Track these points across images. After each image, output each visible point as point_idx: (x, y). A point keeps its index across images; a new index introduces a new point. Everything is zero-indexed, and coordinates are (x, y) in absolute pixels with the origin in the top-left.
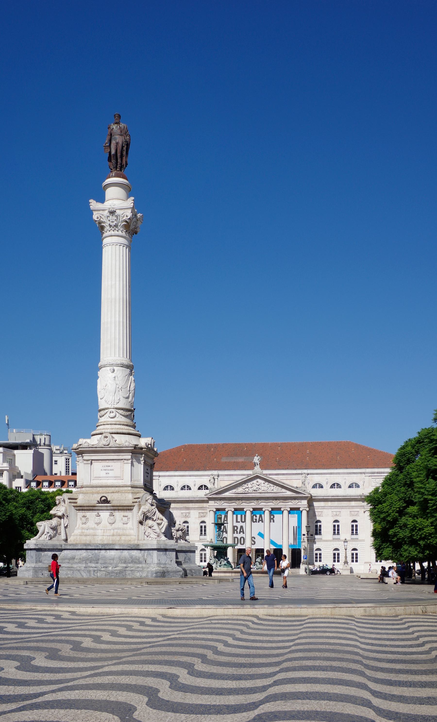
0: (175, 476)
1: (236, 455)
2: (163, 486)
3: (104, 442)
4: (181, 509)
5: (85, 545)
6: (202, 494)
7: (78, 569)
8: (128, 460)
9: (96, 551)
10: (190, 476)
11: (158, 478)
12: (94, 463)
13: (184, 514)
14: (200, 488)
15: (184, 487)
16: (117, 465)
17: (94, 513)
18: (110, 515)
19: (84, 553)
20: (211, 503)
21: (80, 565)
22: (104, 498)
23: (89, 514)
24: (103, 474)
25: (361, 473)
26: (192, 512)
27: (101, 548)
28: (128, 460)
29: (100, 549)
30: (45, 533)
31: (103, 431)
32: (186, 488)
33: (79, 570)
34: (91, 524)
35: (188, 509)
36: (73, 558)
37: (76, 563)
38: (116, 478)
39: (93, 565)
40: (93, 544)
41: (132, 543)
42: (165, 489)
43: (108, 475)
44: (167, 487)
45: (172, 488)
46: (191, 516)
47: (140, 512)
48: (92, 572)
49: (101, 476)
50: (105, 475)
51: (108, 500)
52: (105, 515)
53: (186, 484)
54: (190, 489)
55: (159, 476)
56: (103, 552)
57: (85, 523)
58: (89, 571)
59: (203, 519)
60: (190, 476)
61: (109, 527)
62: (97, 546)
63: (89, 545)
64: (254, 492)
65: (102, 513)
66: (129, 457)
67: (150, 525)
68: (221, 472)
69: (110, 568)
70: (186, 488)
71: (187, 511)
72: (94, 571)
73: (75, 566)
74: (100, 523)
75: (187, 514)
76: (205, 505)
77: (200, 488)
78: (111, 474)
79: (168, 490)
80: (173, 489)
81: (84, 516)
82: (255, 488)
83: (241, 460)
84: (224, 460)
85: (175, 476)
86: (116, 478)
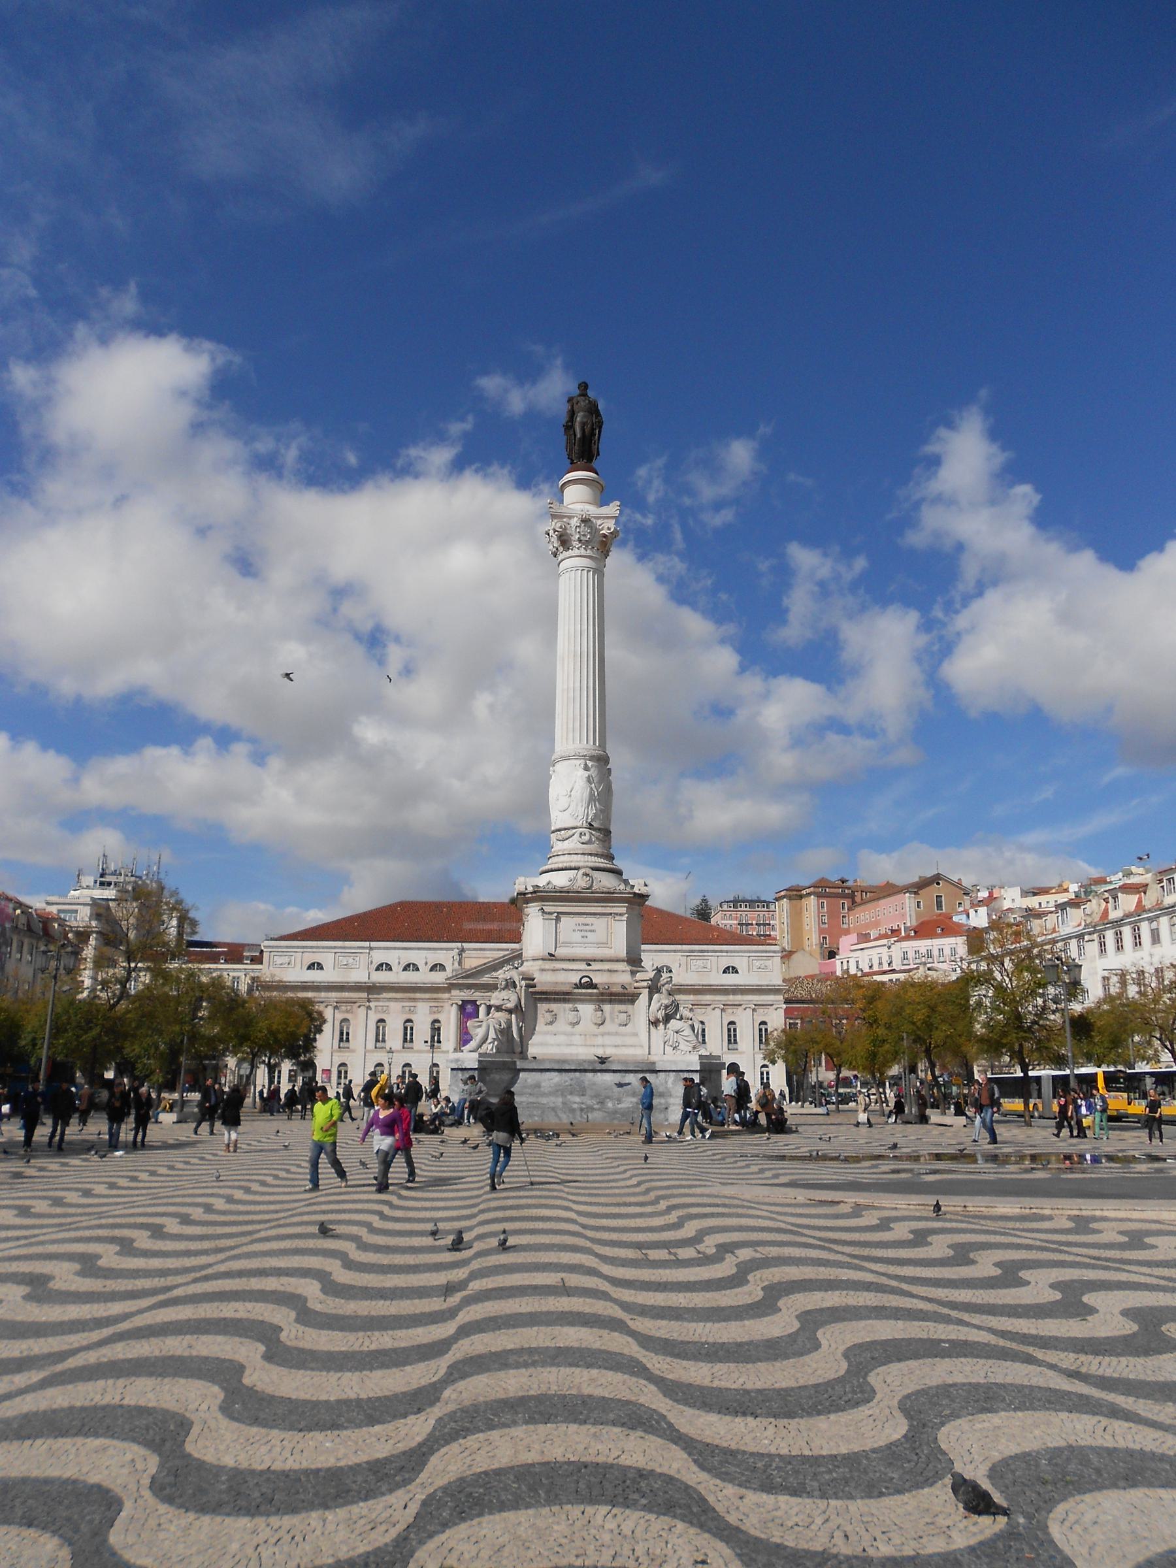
0: (395, 948)
1: (484, 919)
2: (375, 966)
3: (582, 883)
4: (402, 1000)
5: (558, 1061)
6: (439, 978)
7: (552, 1105)
8: (621, 915)
9: (577, 1074)
10: (419, 949)
12: (563, 919)
14: (433, 968)
16: (599, 923)
17: (569, 1006)
18: (596, 1010)
19: (555, 1077)
20: (455, 992)
21: (553, 1099)
22: (584, 980)
23: (554, 1006)
24: (577, 937)
25: (675, 951)
26: (420, 1005)
27: (586, 1067)
28: (621, 915)
29: (585, 1071)
30: (489, 1040)
31: (577, 864)
33: (553, 1109)
34: (561, 1025)
35: (414, 1000)
36: (538, 1086)
37: (544, 1095)
38: (600, 944)
39: (577, 1099)
40: (573, 1061)
41: (640, 1059)
42: (377, 969)
43: (585, 940)
47: (655, 1005)
48: (578, 1113)
49: (573, 940)
50: (580, 940)
51: (594, 981)
52: (587, 1010)
54: (418, 969)
55: (371, 948)
56: (590, 1075)
57: (551, 1023)
58: (573, 1111)
59: (436, 1017)
60: (419, 949)
61: (594, 1029)
62: (580, 1064)
63: (564, 1061)
65: (580, 1006)
66: (624, 910)
67: (676, 1029)
68: (466, 945)
69: (610, 1105)
72: (582, 1110)
73: (544, 1100)
74: (578, 1023)
76: (440, 995)
77: (433, 968)
78: (591, 937)
80: (391, 969)
81: (549, 1011)
83: (493, 926)
84: (467, 926)
85: (395, 948)
86: (600, 944)
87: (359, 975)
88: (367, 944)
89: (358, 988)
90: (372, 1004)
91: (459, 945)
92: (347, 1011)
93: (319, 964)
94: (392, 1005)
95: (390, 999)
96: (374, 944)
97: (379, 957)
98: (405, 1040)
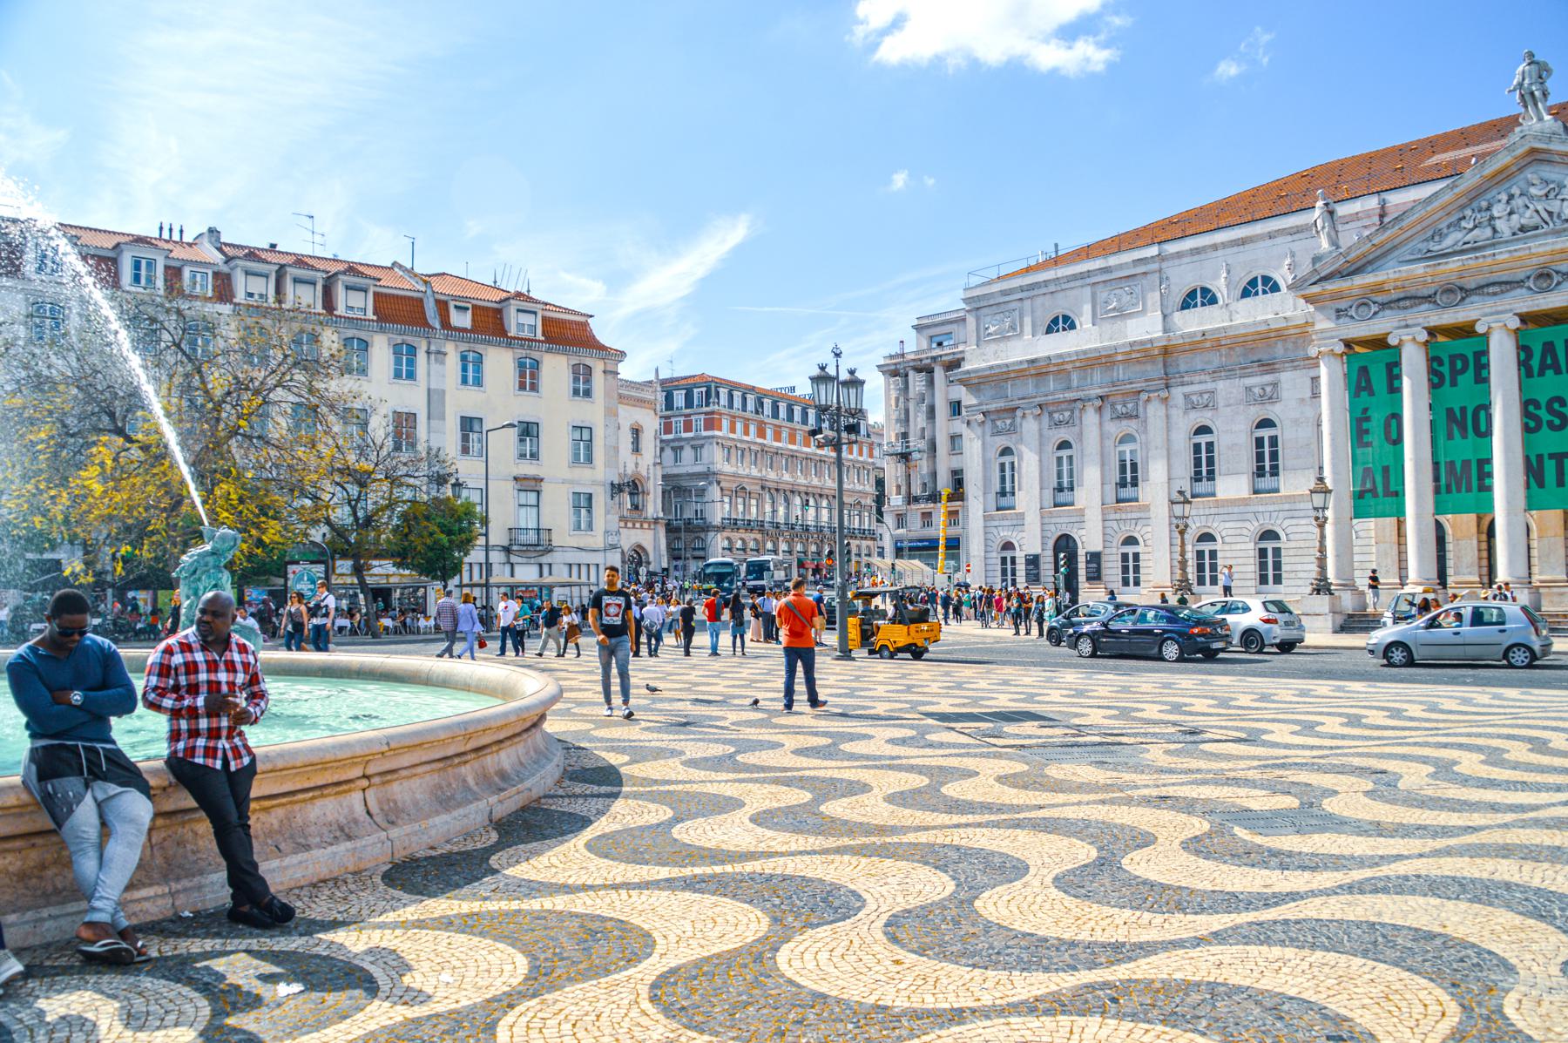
2: (1178, 298)
10: (1271, 236)
11: (1155, 266)
13: (1257, 390)
15: (1253, 283)
32: (1260, 287)
35: (1268, 366)
42: (1185, 305)
44: (1192, 294)
45: (1209, 298)
46: (1285, 395)
53: (1258, 272)
64: (1521, 235)
70: (1260, 287)
71: (1268, 378)
75: (1268, 389)
79: (1195, 306)
80: (1213, 301)
82: (1528, 218)
85: (1215, 247)
87: (1145, 327)
88: (1153, 251)
89: (1141, 353)
90: (1178, 393)
91: (1372, 203)
92: (1128, 416)
93: (1066, 318)
94: (1221, 385)
95: (1216, 373)
96: (1171, 248)
97: (1184, 278)
98: (1260, 472)
